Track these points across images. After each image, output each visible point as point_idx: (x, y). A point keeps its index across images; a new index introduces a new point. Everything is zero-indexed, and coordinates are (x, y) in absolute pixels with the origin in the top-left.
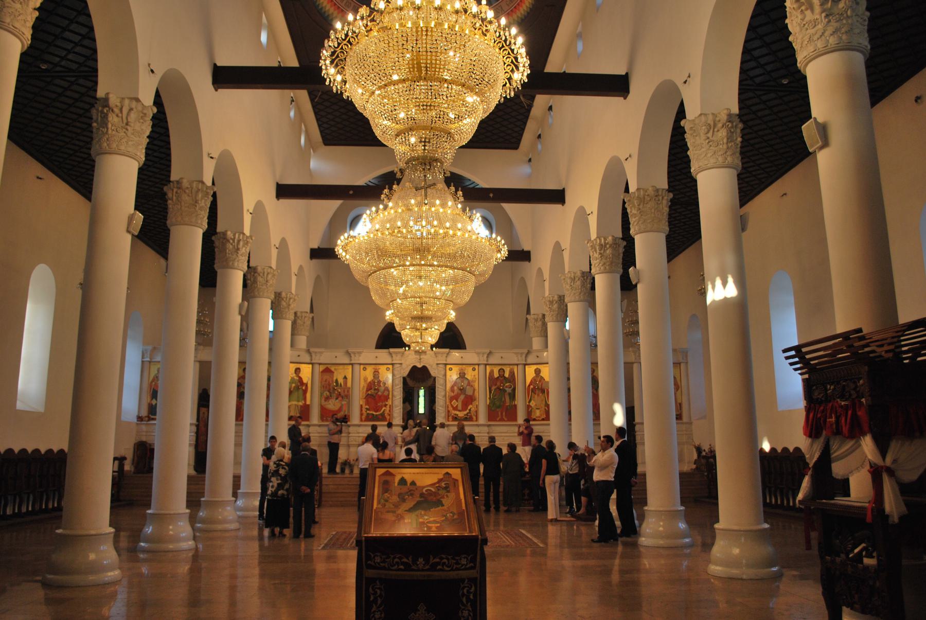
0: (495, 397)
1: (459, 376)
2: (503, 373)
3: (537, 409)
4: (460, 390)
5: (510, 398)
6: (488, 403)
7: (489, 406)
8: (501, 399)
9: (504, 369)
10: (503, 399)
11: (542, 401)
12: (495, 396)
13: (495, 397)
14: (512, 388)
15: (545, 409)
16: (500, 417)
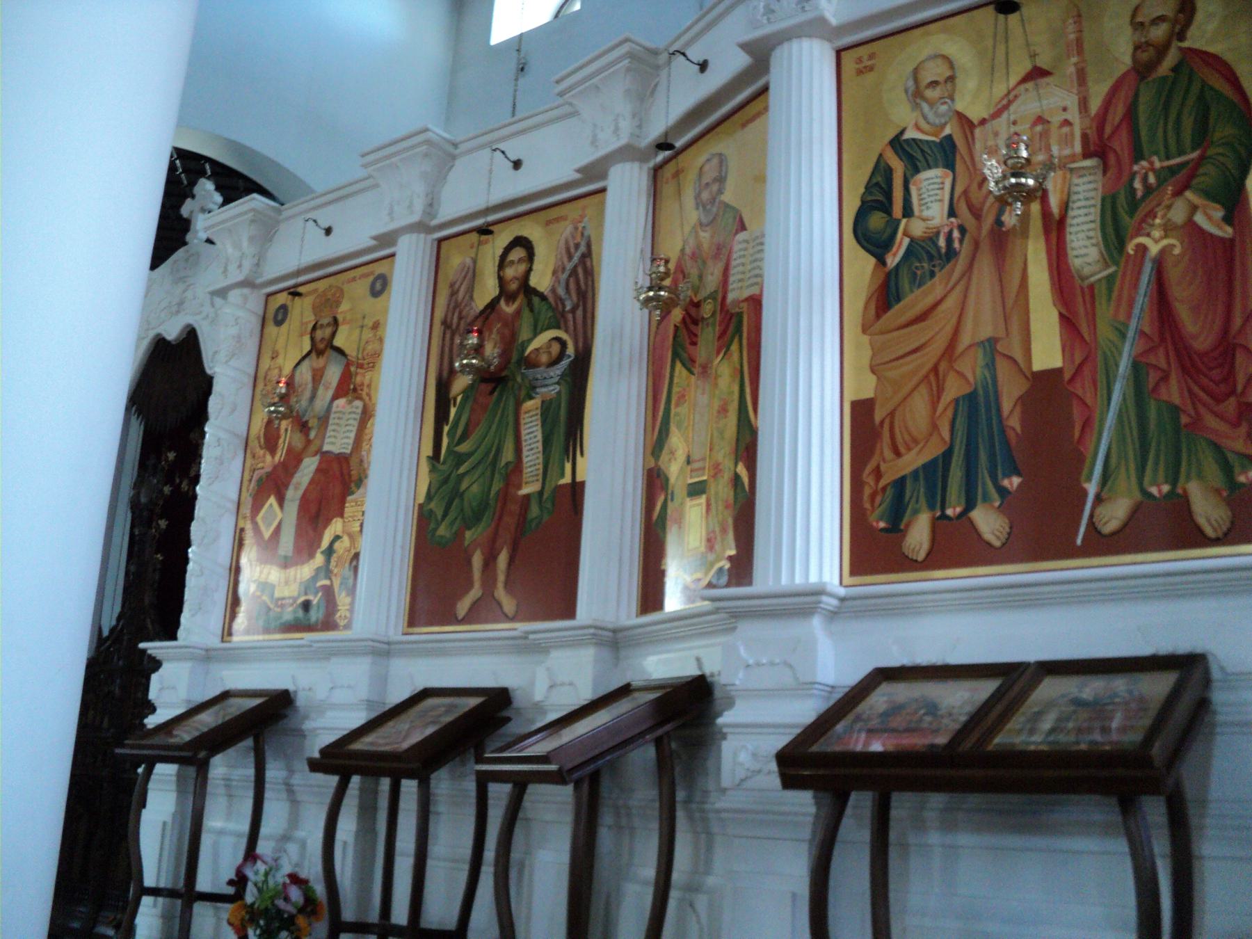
0: (463, 448)
1: (307, 346)
2: (522, 268)
3: (696, 490)
4: (304, 427)
5: (547, 442)
6: (421, 499)
7: (424, 519)
8: (499, 451)
9: (525, 233)
10: (508, 455)
11: (723, 410)
12: (465, 437)
13: (463, 448)
14: (565, 363)
15: (736, 478)
16: (475, 592)
